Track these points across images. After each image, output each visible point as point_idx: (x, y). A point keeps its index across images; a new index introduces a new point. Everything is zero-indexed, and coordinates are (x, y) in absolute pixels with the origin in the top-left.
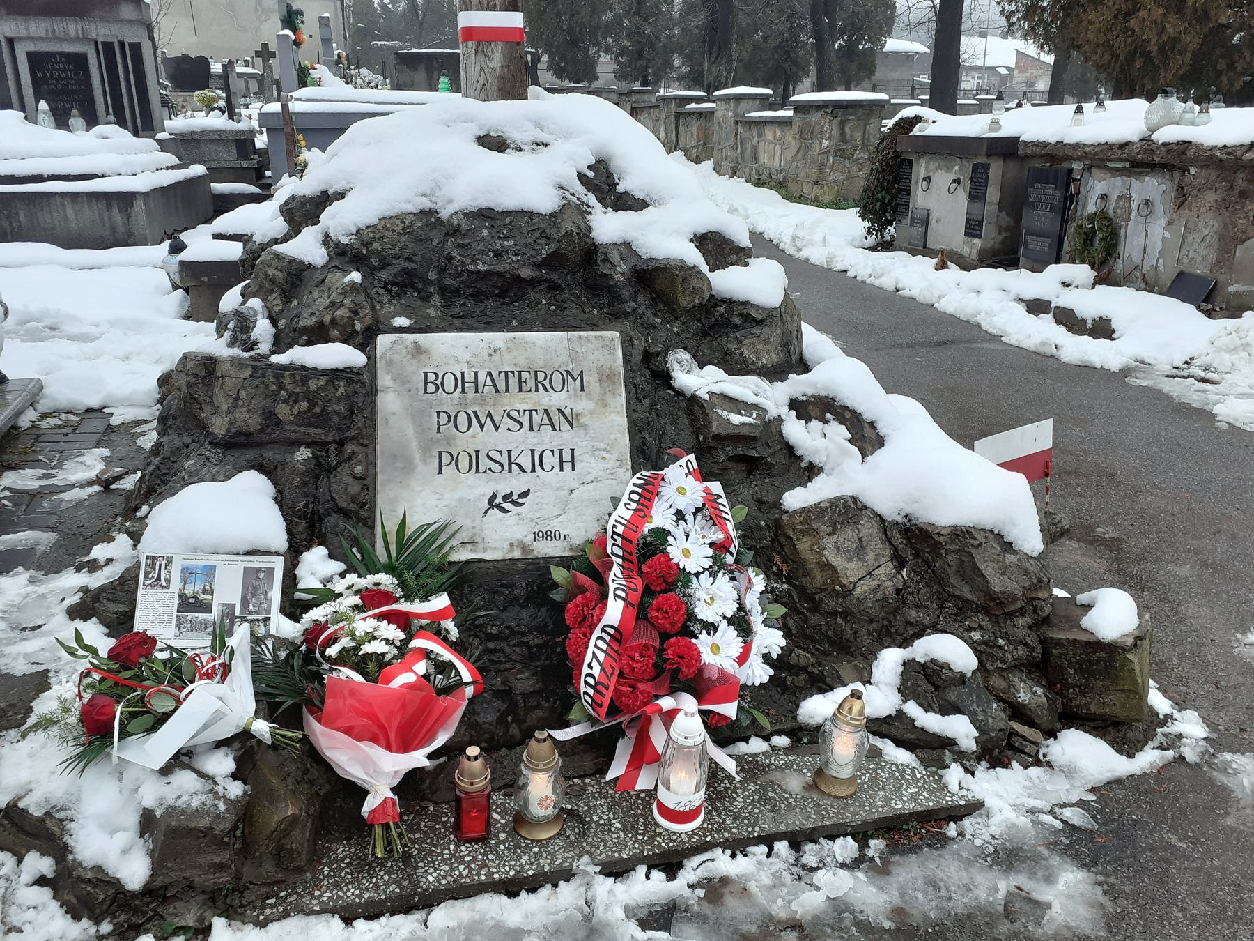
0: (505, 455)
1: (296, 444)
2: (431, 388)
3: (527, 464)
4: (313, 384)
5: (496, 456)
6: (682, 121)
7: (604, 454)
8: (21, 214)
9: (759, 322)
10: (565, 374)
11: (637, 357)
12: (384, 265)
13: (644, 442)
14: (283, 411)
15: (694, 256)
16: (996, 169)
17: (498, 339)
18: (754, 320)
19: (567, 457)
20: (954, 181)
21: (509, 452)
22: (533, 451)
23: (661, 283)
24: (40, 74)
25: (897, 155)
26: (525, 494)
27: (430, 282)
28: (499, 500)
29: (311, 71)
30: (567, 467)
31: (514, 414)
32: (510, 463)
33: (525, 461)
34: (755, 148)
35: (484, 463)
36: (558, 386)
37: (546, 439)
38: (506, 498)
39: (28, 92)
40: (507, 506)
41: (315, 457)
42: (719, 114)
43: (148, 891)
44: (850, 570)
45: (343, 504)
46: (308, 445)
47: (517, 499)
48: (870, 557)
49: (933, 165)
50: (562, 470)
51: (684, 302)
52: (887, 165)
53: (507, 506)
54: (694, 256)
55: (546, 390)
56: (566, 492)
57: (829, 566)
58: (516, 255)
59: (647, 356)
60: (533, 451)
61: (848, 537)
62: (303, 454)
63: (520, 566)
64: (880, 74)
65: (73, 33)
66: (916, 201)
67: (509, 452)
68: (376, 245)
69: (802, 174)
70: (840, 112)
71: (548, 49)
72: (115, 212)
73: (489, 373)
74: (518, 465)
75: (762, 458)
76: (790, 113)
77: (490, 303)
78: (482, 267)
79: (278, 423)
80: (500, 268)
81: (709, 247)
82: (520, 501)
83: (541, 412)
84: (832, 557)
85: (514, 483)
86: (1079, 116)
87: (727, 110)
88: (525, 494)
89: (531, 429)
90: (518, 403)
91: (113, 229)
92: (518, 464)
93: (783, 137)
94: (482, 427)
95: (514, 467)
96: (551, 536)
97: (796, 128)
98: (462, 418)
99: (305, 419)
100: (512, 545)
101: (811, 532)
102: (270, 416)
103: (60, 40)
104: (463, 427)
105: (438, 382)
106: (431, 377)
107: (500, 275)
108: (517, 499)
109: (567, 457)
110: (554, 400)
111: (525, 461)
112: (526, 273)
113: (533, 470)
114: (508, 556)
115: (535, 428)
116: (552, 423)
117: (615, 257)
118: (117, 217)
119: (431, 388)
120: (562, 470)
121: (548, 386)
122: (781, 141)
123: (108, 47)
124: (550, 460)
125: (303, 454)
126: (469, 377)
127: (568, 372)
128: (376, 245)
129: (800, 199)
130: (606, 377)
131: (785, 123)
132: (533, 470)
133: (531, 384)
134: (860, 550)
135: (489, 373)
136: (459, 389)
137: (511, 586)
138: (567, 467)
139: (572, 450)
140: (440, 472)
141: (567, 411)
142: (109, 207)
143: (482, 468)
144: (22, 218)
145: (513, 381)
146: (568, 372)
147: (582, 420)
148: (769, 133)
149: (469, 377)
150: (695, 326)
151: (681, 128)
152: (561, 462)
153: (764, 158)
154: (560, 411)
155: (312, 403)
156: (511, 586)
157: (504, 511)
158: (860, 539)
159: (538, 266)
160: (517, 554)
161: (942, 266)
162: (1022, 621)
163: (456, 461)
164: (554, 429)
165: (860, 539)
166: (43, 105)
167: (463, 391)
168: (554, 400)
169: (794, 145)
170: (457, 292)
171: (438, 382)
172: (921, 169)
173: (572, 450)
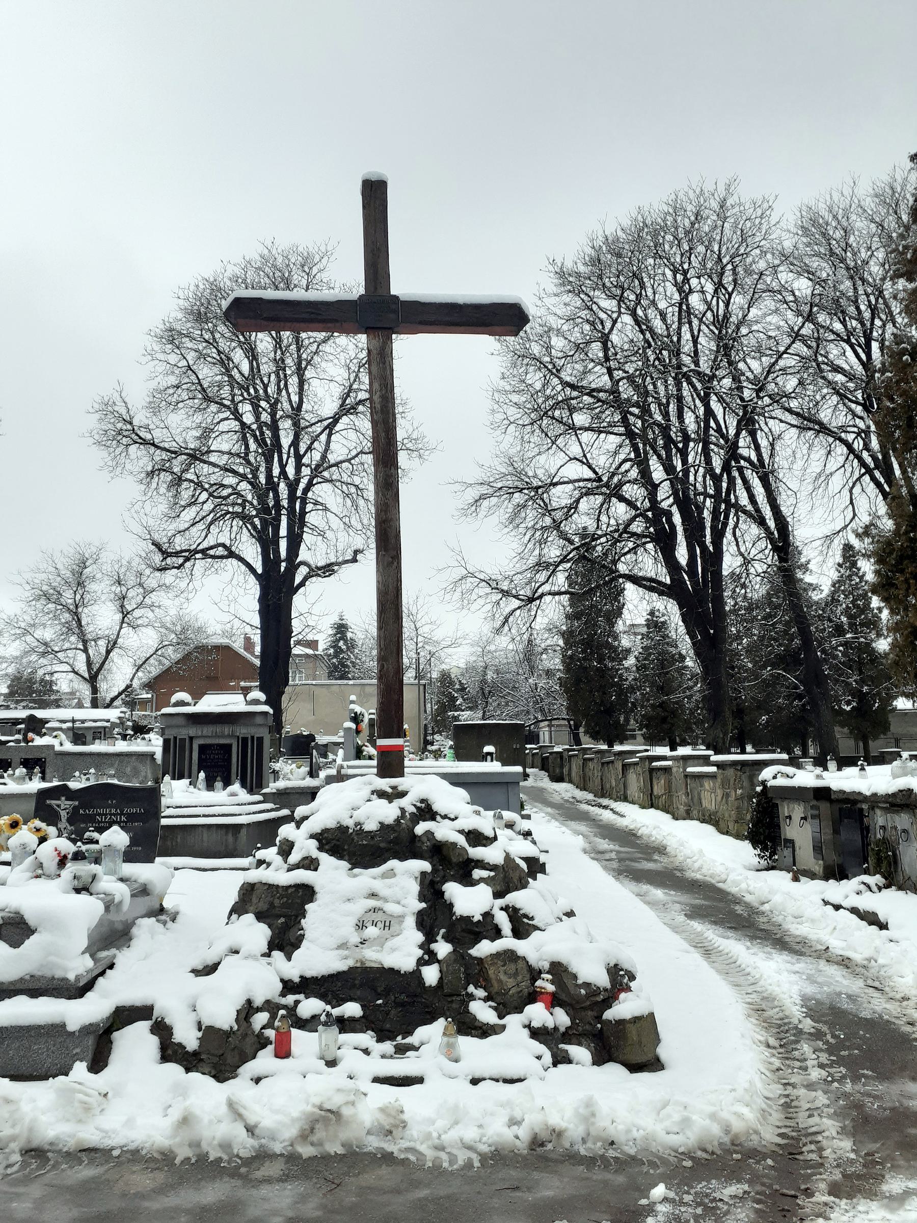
1: (279, 916)
4: (290, 891)
6: (654, 774)
8: (179, 837)
12: (327, 844)
13: (423, 920)
14: (277, 902)
15: (461, 840)
16: (824, 806)
19: (387, 924)
20: (802, 818)
23: (445, 852)
24: (203, 757)
25: (769, 800)
27: (345, 850)
29: (364, 748)
30: (387, 928)
34: (699, 795)
39: (195, 767)
41: (286, 922)
42: (674, 770)
43: (195, 1054)
44: (510, 982)
45: (292, 941)
48: (519, 978)
49: (791, 806)
51: (454, 860)
52: (763, 807)
54: (461, 840)
57: (500, 981)
61: (511, 968)
62: (282, 920)
63: (359, 970)
64: (895, 727)
65: (226, 733)
66: (785, 834)
68: (326, 835)
69: (726, 815)
70: (747, 769)
71: (585, 716)
72: (230, 835)
75: (480, 932)
76: (714, 769)
77: (367, 859)
78: (365, 842)
79: (275, 907)
80: (372, 843)
81: (472, 836)
84: (503, 977)
86: (863, 772)
87: (679, 767)
91: (226, 846)
93: (714, 786)
97: (719, 780)
99: (283, 906)
101: (493, 964)
102: (272, 904)
103: (219, 737)
107: (372, 846)
109: (387, 924)
112: (382, 845)
117: (425, 839)
118: (230, 838)
122: (713, 791)
123: (245, 740)
125: (282, 920)
128: (326, 835)
129: (727, 833)
131: (712, 776)
134: (516, 974)
137: (354, 979)
142: (227, 833)
144: (179, 840)
148: (708, 784)
150: (461, 872)
151: (655, 782)
153: (706, 803)
155: (288, 899)
156: (354, 979)
159: (390, 842)
160: (358, 965)
161: (796, 879)
162: (590, 1013)
166: (202, 775)
169: (719, 792)
170: (354, 854)
172: (785, 809)
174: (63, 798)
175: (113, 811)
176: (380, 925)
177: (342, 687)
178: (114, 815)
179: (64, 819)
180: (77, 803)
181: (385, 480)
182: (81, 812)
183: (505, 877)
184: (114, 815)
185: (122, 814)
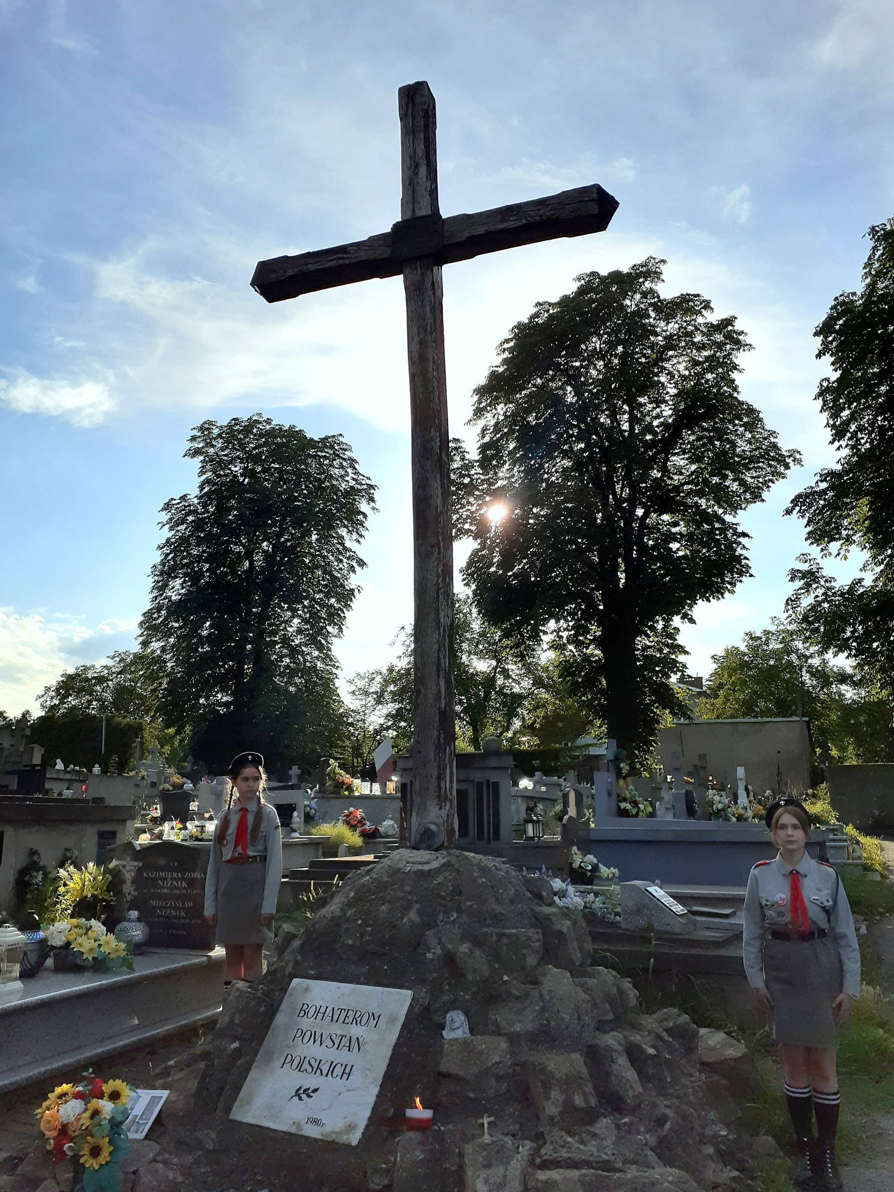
0: (318, 1062)
1: (235, 1038)
2: (303, 1013)
3: (325, 1073)
5: (313, 1062)
7: (367, 1072)
9: (517, 998)
10: (371, 1014)
11: (417, 1010)
17: (346, 987)
18: (514, 996)
19: (347, 1071)
21: (321, 1060)
22: (332, 1062)
26: (315, 1091)
28: (301, 1091)
30: (345, 1076)
31: (334, 1037)
32: (318, 1068)
33: (325, 1069)
35: (306, 1065)
36: (363, 1023)
37: (343, 1056)
38: (305, 1091)
40: (304, 1096)
46: (240, 1039)
47: (309, 1093)
50: (341, 1078)
53: (304, 1096)
55: (356, 1024)
56: (337, 1094)
58: (370, 936)
59: (427, 1009)
60: (332, 1062)
62: (236, 1045)
67: (321, 1060)
73: (333, 1009)
74: (321, 1070)
78: (350, 942)
82: (311, 1094)
83: (348, 1038)
85: (310, 1081)
88: (315, 1091)
89: (338, 1048)
90: (337, 1029)
92: (321, 1070)
94: (314, 1042)
95: (319, 1071)
96: (316, 1122)
98: (308, 1034)
100: (294, 1123)
104: (305, 1040)
105: (307, 1011)
106: (305, 1006)
108: (309, 1093)
109: (347, 1071)
110: (356, 1031)
111: (325, 1069)
113: (327, 1076)
114: (289, 1130)
115: (340, 1048)
116: (349, 1047)
119: (303, 1013)
120: (341, 1078)
121: (356, 1021)
124: (338, 1071)
125: (236, 1045)
126: (323, 1010)
127: (373, 1014)
130: (392, 1020)
132: (327, 1076)
133: (351, 1018)
135: (333, 1009)
136: (314, 1017)
138: (345, 1076)
139: (352, 1066)
140: (282, 1067)
141: (361, 1040)
143: (302, 1070)
145: (343, 1014)
146: (373, 1014)
147: (367, 1047)
149: (323, 1010)
152: (344, 1072)
154: (358, 1039)
157: (301, 1099)
158: (505, 1176)
160: (293, 1130)
163: (292, 1061)
164: (349, 1050)
165: (505, 1176)
167: (315, 1018)
168: (356, 1031)
171: (307, 1011)
173: (352, 1066)
174: (128, 859)
175: (175, 875)
176: (338, 1071)
177: (713, 726)
178: (175, 879)
179: (128, 883)
180: (141, 864)
181: (424, 446)
182: (145, 875)
183: (543, 1010)
184: (175, 879)
185: (183, 879)
